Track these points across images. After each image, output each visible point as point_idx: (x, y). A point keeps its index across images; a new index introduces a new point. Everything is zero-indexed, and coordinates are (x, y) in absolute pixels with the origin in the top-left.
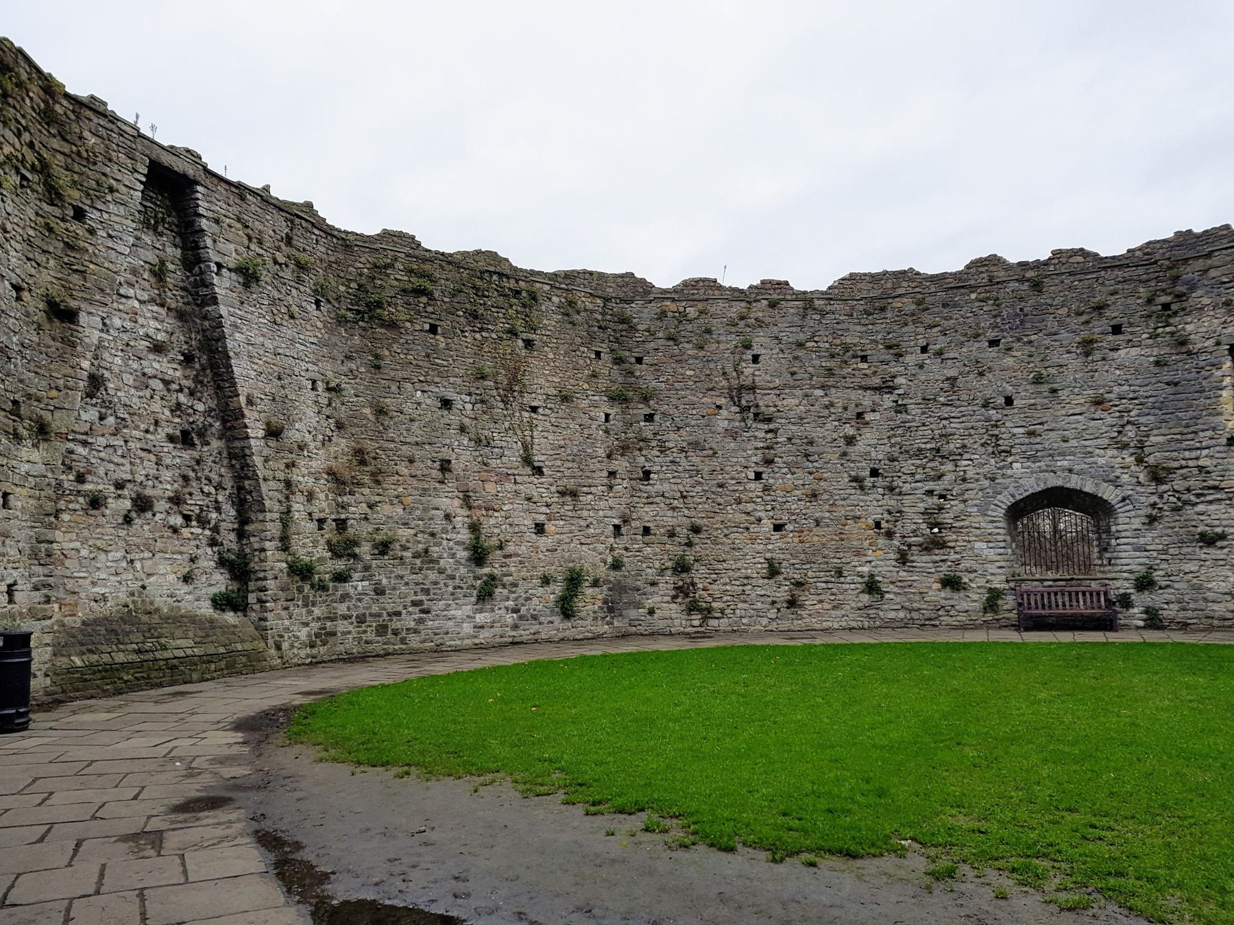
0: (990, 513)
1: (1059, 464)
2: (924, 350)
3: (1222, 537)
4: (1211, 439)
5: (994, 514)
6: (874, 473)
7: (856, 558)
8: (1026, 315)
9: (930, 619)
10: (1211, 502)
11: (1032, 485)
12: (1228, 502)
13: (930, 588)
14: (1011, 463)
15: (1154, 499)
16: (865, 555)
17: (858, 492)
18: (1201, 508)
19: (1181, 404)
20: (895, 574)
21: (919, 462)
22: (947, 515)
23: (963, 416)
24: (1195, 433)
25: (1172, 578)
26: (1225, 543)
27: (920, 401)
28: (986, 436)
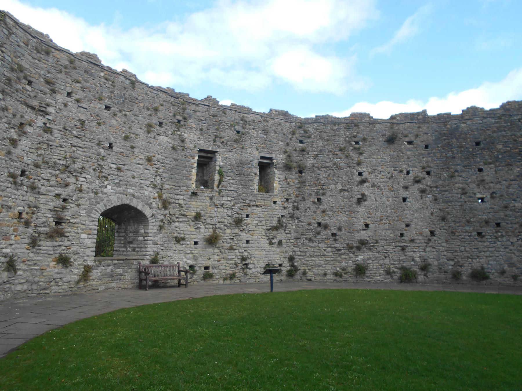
0: (92, 215)
1: (129, 190)
2: (69, 94)
3: (183, 239)
4: (185, 191)
5: (94, 216)
6: (23, 173)
7: (4, 242)
8: (126, 99)
9: (44, 289)
10: (181, 222)
11: (115, 201)
12: (188, 223)
13: (48, 265)
14: (107, 186)
15: (162, 217)
16: (9, 239)
17: (13, 186)
18: (177, 224)
19: (177, 171)
20: (26, 255)
21: (53, 172)
22: (67, 213)
23: (86, 148)
24: (180, 187)
25: (164, 259)
26: (184, 242)
27: (62, 129)
28: (96, 165)
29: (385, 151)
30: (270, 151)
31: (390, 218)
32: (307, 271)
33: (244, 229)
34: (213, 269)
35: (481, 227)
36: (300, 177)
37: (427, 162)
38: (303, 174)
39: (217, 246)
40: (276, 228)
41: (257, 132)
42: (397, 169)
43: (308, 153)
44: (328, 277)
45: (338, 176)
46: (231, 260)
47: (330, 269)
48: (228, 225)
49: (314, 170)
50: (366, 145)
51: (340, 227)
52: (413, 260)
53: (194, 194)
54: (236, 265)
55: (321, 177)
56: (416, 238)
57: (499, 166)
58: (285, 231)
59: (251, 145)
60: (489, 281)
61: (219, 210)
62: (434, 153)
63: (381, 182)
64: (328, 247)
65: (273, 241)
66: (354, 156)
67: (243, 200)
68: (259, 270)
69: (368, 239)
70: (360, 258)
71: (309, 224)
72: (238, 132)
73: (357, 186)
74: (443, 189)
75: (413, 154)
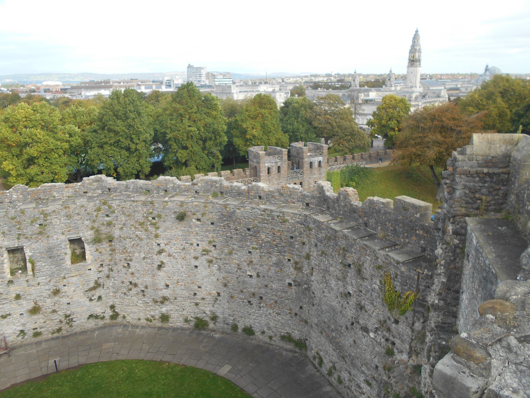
29: (177, 226)
30: (77, 232)
31: (185, 281)
32: (126, 315)
33: (63, 296)
34: (41, 328)
35: (250, 297)
36: (110, 246)
37: (213, 237)
38: (113, 243)
39: (41, 312)
40: (94, 288)
41: (60, 220)
42: (189, 242)
43: (115, 227)
44: (142, 321)
45: (141, 247)
46: (55, 319)
47: (142, 316)
48: (48, 296)
49: (121, 240)
50: (161, 221)
51: (146, 285)
52: (205, 313)
53: (10, 282)
54: (61, 322)
55: (127, 246)
56: (206, 297)
57: (263, 253)
58: (103, 288)
59: (56, 232)
60: (254, 336)
61: (36, 288)
62: (218, 230)
63: (175, 253)
64: (139, 300)
65: (93, 298)
66: (152, 230)
67: (58, 275)
68: (83, 320)
69: (169, 296)
70: (164, 310)
71: (123, 282)
72: (41, 225)
73: (156, 255)
74: (225, 262)
75: (201, 230)
